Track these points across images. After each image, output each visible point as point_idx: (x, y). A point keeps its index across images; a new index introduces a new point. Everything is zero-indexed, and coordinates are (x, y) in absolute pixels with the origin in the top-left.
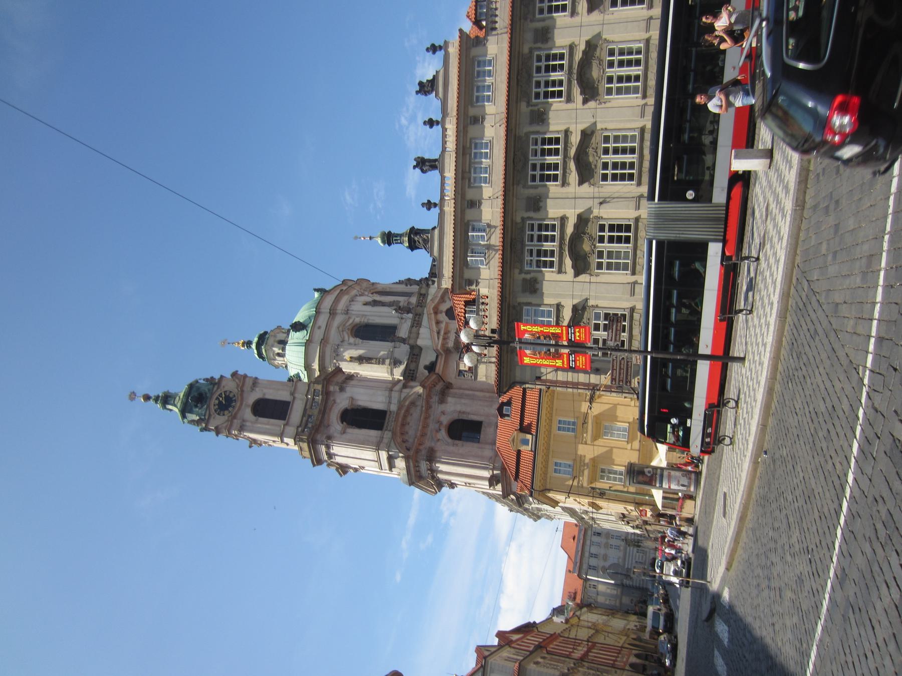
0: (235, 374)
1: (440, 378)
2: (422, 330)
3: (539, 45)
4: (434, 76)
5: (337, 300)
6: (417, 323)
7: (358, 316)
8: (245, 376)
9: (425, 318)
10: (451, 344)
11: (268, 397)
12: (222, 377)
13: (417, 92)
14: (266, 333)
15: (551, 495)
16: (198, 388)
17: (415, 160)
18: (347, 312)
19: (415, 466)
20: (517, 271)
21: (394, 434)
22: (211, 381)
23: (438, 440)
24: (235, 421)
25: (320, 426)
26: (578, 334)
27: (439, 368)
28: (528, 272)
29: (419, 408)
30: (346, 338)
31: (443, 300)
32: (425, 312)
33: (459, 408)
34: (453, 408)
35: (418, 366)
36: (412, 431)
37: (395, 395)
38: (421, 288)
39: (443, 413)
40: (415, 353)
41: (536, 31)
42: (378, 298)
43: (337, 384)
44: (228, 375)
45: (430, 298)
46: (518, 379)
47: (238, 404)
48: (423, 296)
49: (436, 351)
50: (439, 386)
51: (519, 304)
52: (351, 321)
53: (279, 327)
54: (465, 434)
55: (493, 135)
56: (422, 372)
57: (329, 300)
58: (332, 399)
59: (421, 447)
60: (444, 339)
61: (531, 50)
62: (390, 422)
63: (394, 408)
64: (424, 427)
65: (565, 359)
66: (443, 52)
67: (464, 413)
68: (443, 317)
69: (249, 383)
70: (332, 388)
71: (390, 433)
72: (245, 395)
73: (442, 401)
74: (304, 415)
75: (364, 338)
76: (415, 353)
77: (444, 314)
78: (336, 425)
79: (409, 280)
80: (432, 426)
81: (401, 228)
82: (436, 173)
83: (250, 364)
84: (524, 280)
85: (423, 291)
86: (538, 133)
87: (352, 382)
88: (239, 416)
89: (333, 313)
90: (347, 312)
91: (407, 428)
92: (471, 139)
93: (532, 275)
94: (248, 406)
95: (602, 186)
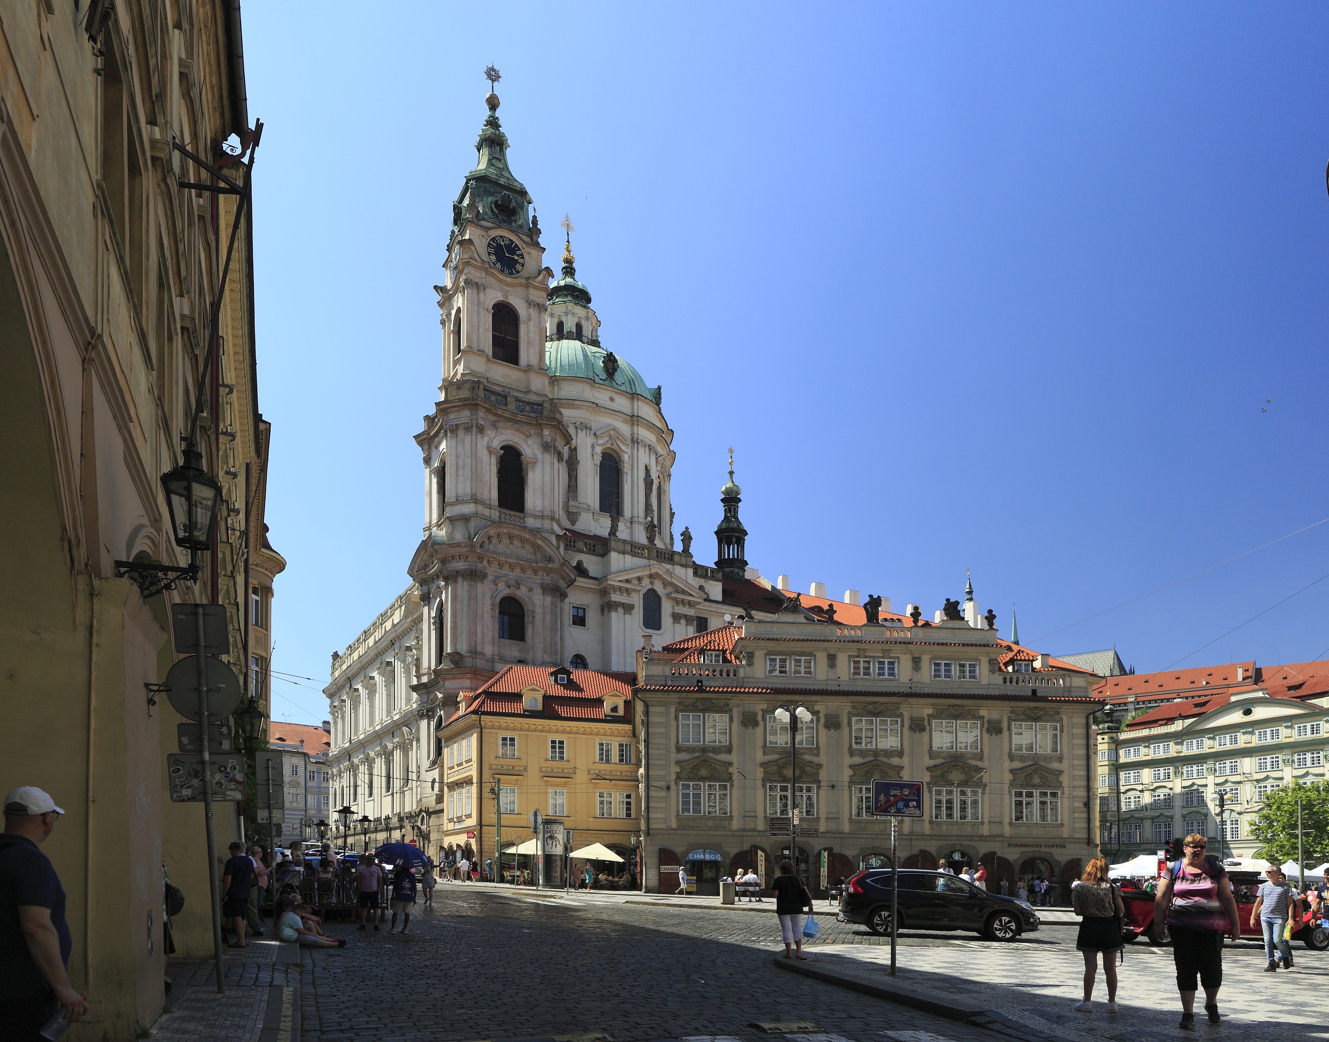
2: (628, 558)
5: (650, 426)
6: (634, 549)
7: (632, 458)
9: (644, 562)
20: (765, 707)
21: (499, 523)
27: (581, 581)
32: (652, 562)
37: (547, 524)
38: (679, 553)
42: (655, 487)
45: (669, 567)
47: (508, 279)
48: (668, 557)
49: (605, 578)
50: (562, 584)
52: (624, 448)
56: (575, 558)
60: (620, 588)
63: (531, 522)
68: (646, 585)
77: (650, 587)
81: (745, 515)
82: (864, 620)
85: (676, 558)
90: (635, 441)
92: (898, 658)
94: (506, 295)
95: (764, 786)
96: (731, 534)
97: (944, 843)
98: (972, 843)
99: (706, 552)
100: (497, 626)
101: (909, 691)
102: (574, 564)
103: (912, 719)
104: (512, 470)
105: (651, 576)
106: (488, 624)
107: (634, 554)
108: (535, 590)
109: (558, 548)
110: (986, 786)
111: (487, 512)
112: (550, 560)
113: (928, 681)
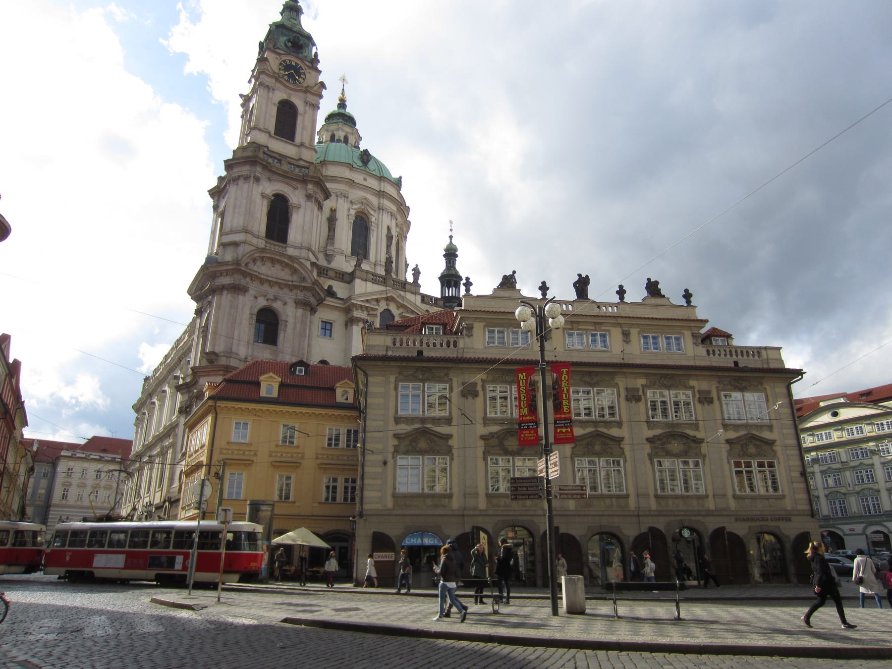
0: (323, 85)
1: (320, 302)
2: (369, 284)
3: (697, 396)
4: (664, 296)
6: (375, 278)
8: (321, 97)
9: (382, 288)
10: (357, 314)
11: (300, 119)
12: (320, 72)
13: (649, 279)
14: (354, 124)
15: (210, 419)
16: (308, 46)
17: (587, 276)
18: (381, 209)
19: (227, 271)
21: (263, 250)
22: (315, 60)
23: (256, 297)
24: (274, 81)
25: (270, 171)
26: (564, 430)
27: (329, 301)
28: (484, 389)
29: (290, 278)
30: (355, 207)
31: (400, 306)
33: (291, 320)
34: (290, 313)
35: (332, 279)
36: (265, 270)
37: (304, 253)
38: (410, 283)
39: (285, 304)
40: (348, 278)
41: (709, 392)
43: (316, 193)
44: (321, 78)
45: (402, 293)
46: (370, 379)
49: (350, 298)
50: (313, 300)
51: (451, 379)
52: (372, 212)
53: (360, 139)
54: (262, 326)
55: (614, 352)
57: (390, 190)
58: (299, 186)
59: (248, 279)
60: (361, 306)
61: (692, 388)
62: (275, 246)
63: (290, 251)
64: (270, 281)
65: (528, 418)
66: (685, 305)
67: (286, 326)
68: (383, 306)
69: (311, 98)
70: (310, 186)
71: (263, 246)
72: (301, 95)
73: (298, 303)
74: (280, 155)
75: (355, 223)
76: (348, 278)
78: (271, 188)
79: (419, 273)
80: (272, 292)
83: (328, 105)
84: (475, 384)
85: (408, 287)
86: (619, 395)
87: (316, 209)
88: (278, 85)
89: (381, 194)
90: (381, 209)
91: (269, 264)
92: (609, 331)
93: (481, 393)
96: (450, 278)
97: (672, 518)
98: (700, 518)
99: (431, 287)
100: (253, 330)
101: (622, 362)
102: (326, 288)
103: (627, 389)
104: (279, 215)
105: (387, 299)
106: (245, 329)
107: (374, 282)
108: (289, 304)
109: (312, 272)
110: (705, 456)
111: (254, 241)
112: (304, 279)
113: (638, 353)
